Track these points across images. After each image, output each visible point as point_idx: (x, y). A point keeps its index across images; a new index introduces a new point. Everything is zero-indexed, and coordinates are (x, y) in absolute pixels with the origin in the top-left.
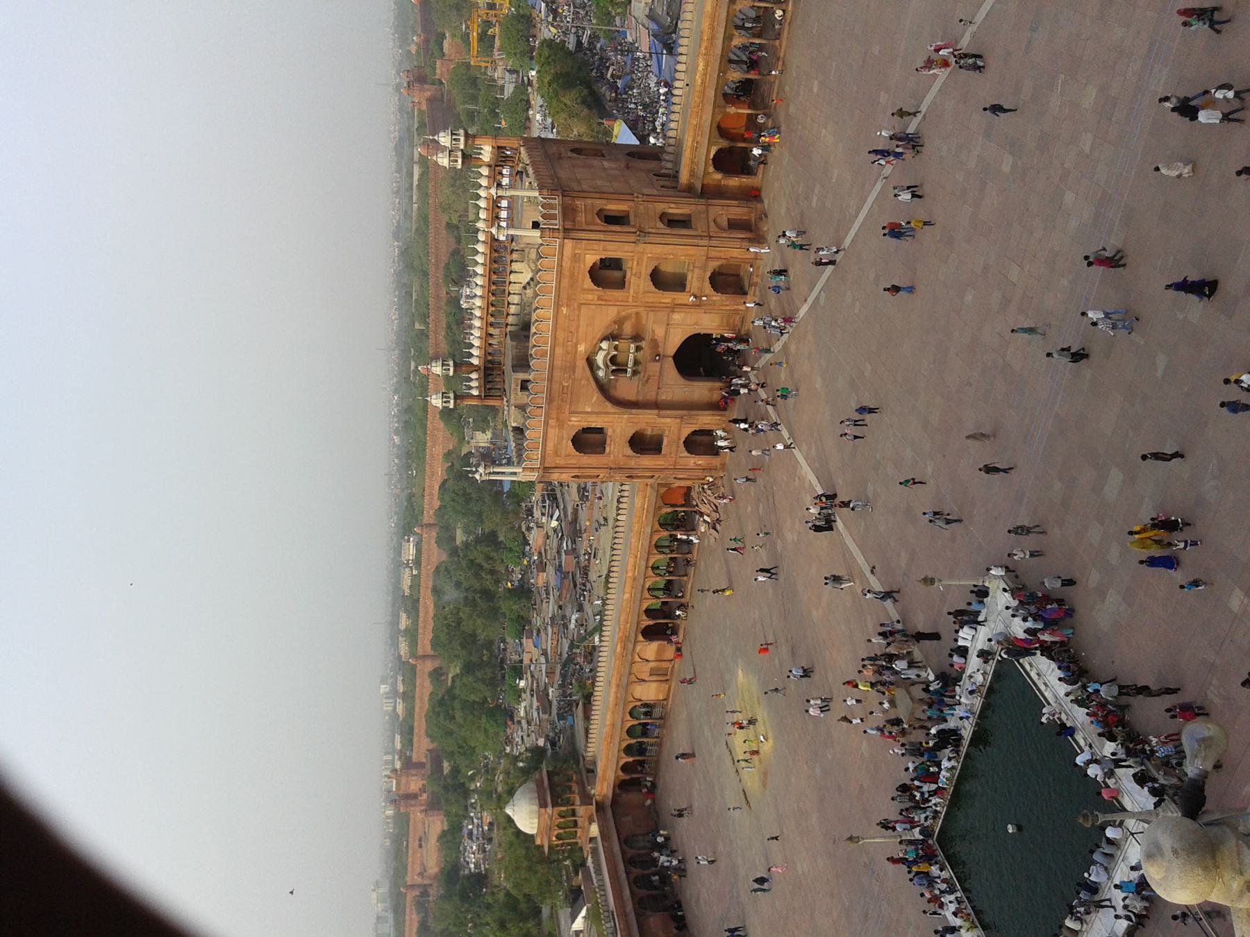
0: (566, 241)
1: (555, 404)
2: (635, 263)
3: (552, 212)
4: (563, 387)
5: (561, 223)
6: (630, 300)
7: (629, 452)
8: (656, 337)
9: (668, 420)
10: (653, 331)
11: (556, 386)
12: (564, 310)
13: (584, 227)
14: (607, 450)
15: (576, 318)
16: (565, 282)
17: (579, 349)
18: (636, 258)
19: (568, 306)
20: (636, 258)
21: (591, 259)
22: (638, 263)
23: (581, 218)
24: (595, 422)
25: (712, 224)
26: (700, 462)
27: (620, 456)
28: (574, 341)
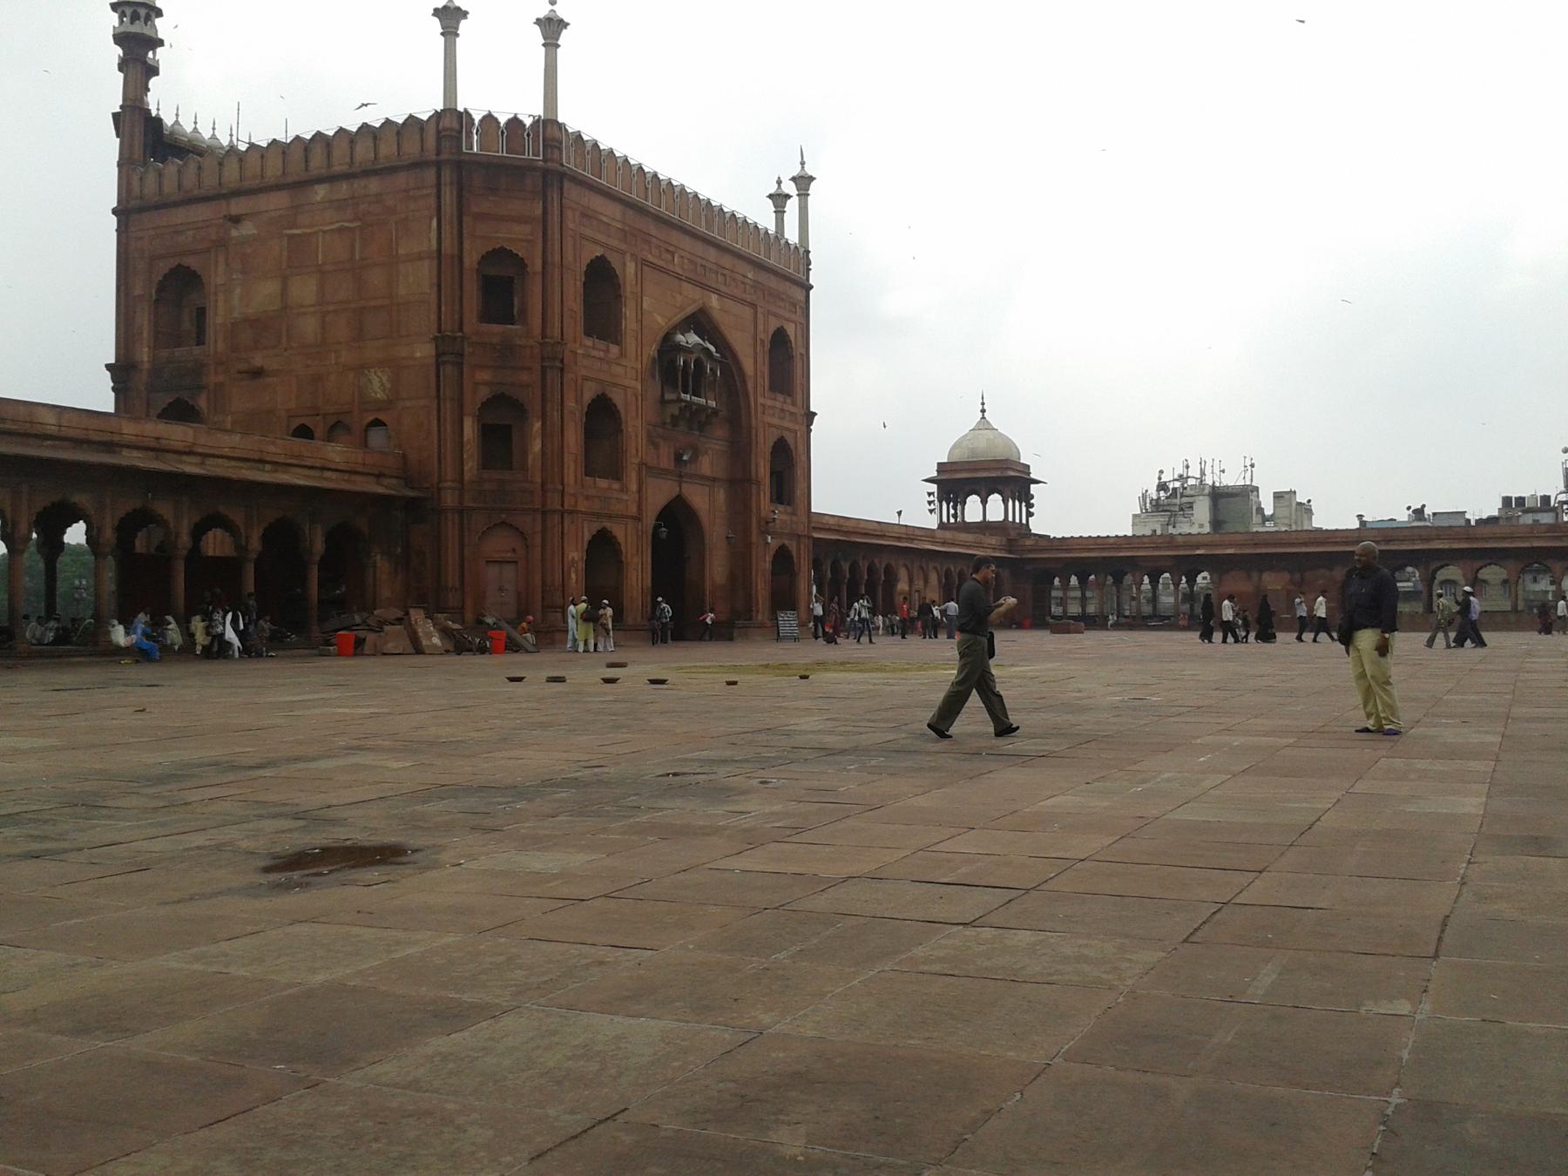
4: (673, 254)
7: (588, 396)
8: (700, 459)
14: (589, 342)
20: (793, 409)
21: (790, 330)
26: (573, 576)
27: (584, 372)
28: (723, 288)
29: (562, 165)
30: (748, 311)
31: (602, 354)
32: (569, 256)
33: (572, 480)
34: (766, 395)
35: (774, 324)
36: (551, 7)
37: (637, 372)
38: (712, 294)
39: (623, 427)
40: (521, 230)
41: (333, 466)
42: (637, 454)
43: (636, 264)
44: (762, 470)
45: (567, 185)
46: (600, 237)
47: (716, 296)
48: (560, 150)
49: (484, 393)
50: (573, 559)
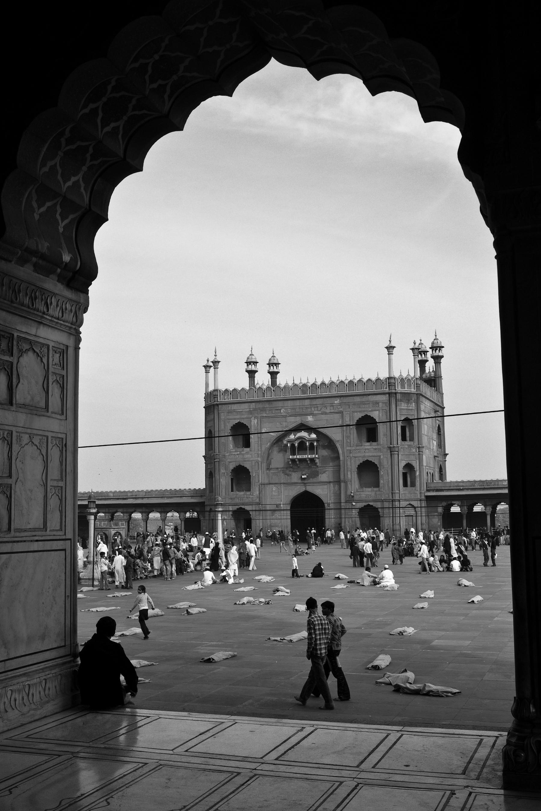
0: (388, 395)
1: (267, 405)
2: (376, 447)
3: (406, 386)
4: (280, 410)
5: (399, 391)
6: (348, 448)
7: (232, 467)
8: (320, 475)
9: (258, 493)
10: (324, 472)
11: (280, 404)
12: (337, 401)
15: (332, 411)
16: (358, 399)
17: (309, 417)
18: (379, 447)
19: (340, 404)
20: (379, 447)
21: (376, 415)
23: (403, 406)
25: (408, 503)
27: (229, 460)
29: (218, 402)
31: (238, 453)
32: (222, 427)
34: (352, 445)
36: (215, 357)
37: (258, 455)
38: (308, 416)
39: (251, 474)
41: (186, 496)
42: (259, 482)
44: (349, 476)
45: (220, 406)
46: (238, 417)
47: (311, 416)
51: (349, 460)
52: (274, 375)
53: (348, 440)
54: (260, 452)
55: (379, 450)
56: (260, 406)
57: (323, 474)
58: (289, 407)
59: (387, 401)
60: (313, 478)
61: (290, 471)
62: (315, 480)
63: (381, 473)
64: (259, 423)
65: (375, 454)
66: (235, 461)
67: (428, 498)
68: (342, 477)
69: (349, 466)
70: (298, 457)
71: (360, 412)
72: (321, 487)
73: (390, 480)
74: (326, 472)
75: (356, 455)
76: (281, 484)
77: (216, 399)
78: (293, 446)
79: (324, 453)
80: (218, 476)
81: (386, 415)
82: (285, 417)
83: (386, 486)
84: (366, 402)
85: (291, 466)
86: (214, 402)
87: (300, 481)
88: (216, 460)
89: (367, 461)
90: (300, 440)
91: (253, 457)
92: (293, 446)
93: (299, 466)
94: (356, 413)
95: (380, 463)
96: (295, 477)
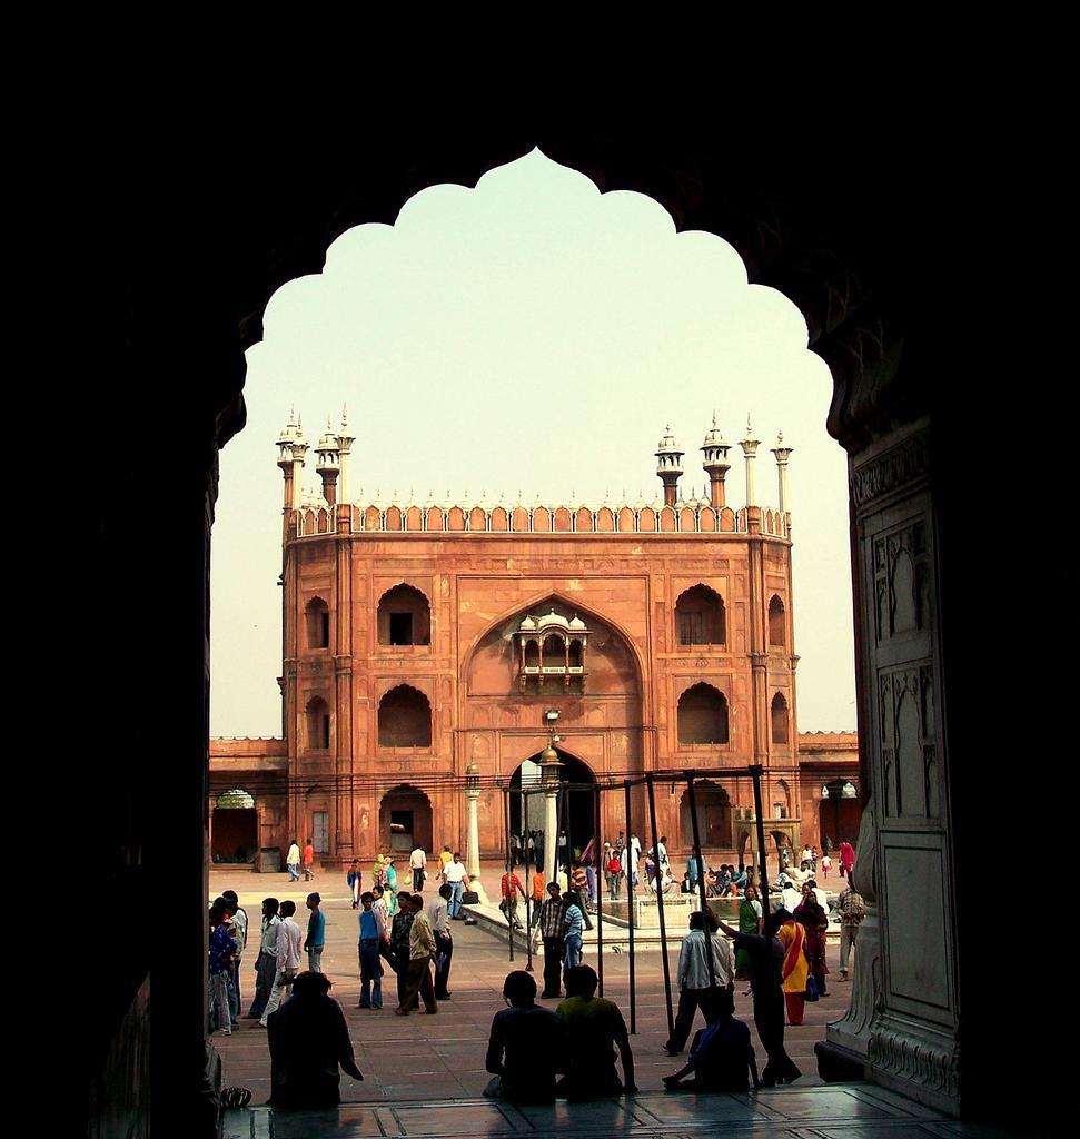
0: (746, 545)
1: (471, 549)
2: (721, 655)
4: (505, 561)
6: (661, 655)
7: (384, 687)
8: (586, 714)
9: (447, 750)
11: (504, 548)
12: (637, 550)
13: (765, 572)
15: (625, 571)
16: (682, 549)
18: (728, 655)
19: (644, 558)
20: (728, 655)
21: (719, 585)
22: (720, 659)
24: (439, 623)
26: (365, 821)
30: (639, 583)
31: (401, 656)
32: (360, 591)
33: (363, 751)
34: (669, 649)
35: (683, 585)
37: (450, 662)
40: (324, 584)
43: (449, 582)
48: (350, 523)
49: (308, 698)
50: (363, 809)
51: (663, 681)
52: (329, 476)
53: (661, 639)
54: (455, 657)
55: (729, 662)
56: (456, 549)
57: (593, 710)
58: (528, 558)
59: (743, 558)
60: (569, 719)
61: (516, 702)
62: (575, 723)
63: (733, 711)
64: (454, 589)
65: (721, 671)
66: (394, 676)
67: (804, 767)
68: (646, 720)
69: (663, 696)
70: (544, 672)
71: (686, 577)
72: (588, 739)
73: (751, 727)
74: (601, 707)
75: (677, 671)
76: (494, 730)
77: (345, 527)
78: (532, 645)
79: (603, 664)
80: (349, 709)
81: (744, 587)
82: (517, 578)
83: (743, 740)
84: (700, 558)
85: (523, 690)
86: (337, 533)
87: (540, 725)
88: (344, 671)
89: (702, 685)
90: (550, 633)
91: (438, 666)
92: (532, 645)
93: (567, 690)
94: (677, 580)
95: (730, 690)
96: (529, 716)
